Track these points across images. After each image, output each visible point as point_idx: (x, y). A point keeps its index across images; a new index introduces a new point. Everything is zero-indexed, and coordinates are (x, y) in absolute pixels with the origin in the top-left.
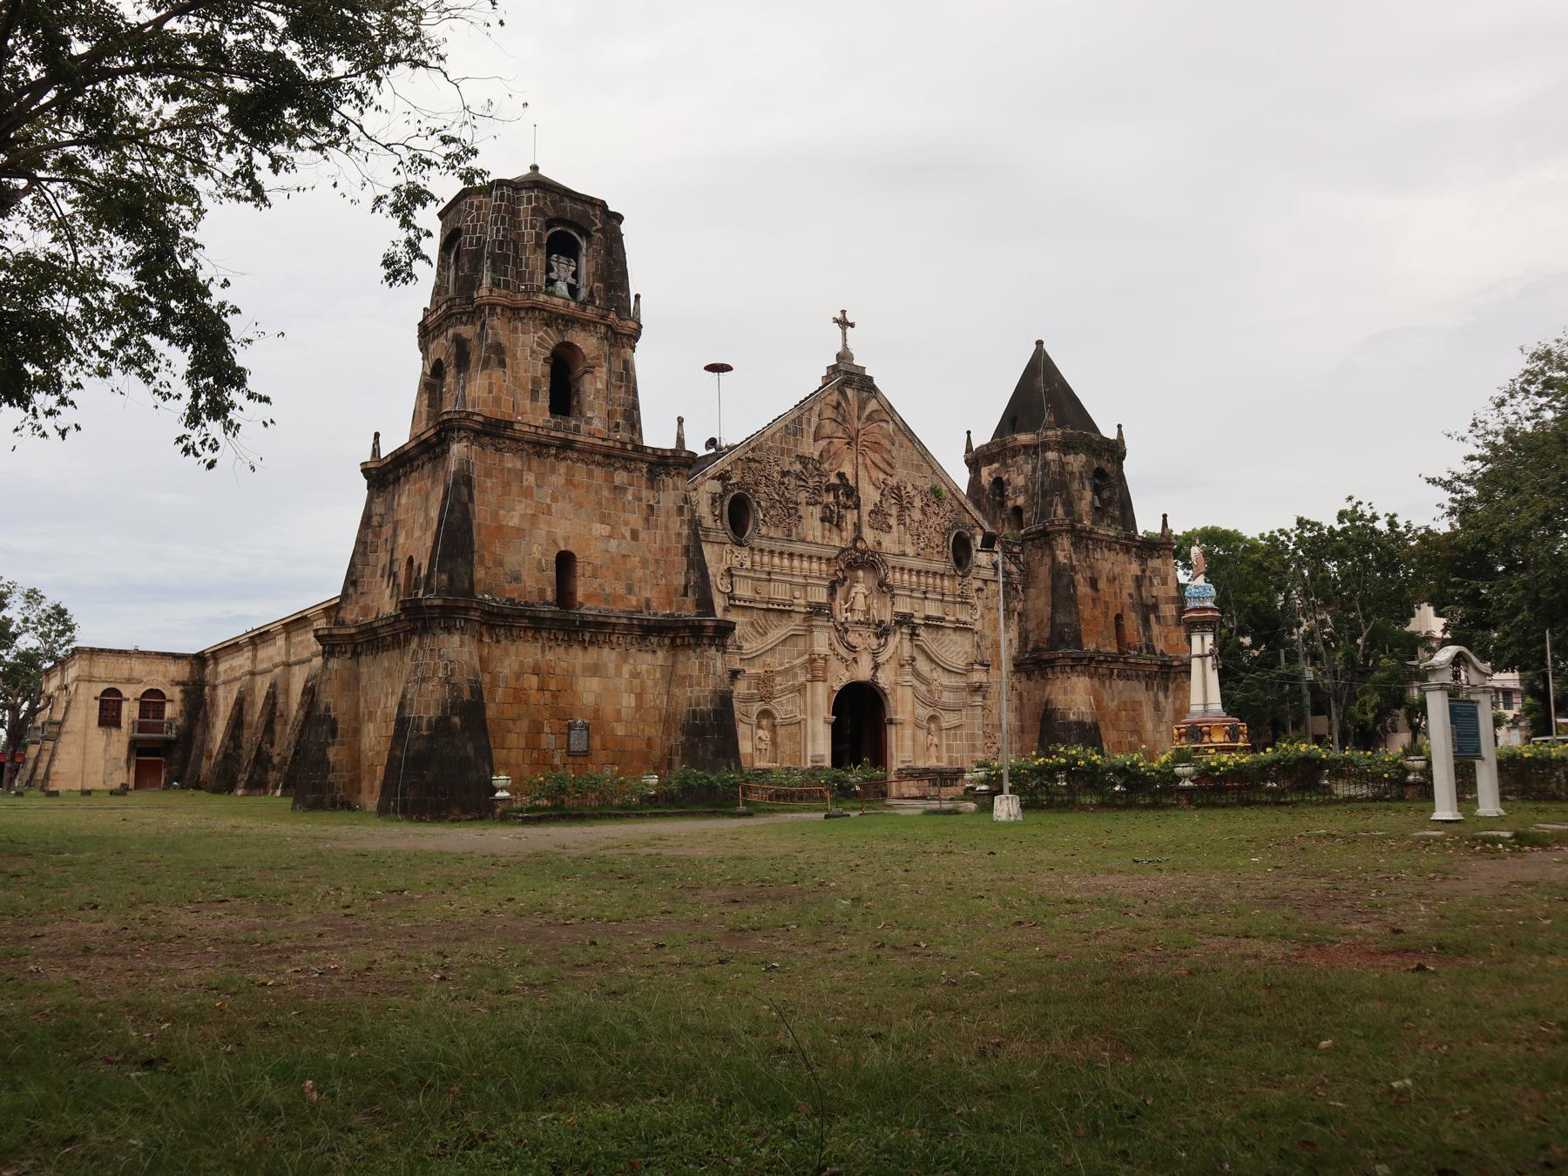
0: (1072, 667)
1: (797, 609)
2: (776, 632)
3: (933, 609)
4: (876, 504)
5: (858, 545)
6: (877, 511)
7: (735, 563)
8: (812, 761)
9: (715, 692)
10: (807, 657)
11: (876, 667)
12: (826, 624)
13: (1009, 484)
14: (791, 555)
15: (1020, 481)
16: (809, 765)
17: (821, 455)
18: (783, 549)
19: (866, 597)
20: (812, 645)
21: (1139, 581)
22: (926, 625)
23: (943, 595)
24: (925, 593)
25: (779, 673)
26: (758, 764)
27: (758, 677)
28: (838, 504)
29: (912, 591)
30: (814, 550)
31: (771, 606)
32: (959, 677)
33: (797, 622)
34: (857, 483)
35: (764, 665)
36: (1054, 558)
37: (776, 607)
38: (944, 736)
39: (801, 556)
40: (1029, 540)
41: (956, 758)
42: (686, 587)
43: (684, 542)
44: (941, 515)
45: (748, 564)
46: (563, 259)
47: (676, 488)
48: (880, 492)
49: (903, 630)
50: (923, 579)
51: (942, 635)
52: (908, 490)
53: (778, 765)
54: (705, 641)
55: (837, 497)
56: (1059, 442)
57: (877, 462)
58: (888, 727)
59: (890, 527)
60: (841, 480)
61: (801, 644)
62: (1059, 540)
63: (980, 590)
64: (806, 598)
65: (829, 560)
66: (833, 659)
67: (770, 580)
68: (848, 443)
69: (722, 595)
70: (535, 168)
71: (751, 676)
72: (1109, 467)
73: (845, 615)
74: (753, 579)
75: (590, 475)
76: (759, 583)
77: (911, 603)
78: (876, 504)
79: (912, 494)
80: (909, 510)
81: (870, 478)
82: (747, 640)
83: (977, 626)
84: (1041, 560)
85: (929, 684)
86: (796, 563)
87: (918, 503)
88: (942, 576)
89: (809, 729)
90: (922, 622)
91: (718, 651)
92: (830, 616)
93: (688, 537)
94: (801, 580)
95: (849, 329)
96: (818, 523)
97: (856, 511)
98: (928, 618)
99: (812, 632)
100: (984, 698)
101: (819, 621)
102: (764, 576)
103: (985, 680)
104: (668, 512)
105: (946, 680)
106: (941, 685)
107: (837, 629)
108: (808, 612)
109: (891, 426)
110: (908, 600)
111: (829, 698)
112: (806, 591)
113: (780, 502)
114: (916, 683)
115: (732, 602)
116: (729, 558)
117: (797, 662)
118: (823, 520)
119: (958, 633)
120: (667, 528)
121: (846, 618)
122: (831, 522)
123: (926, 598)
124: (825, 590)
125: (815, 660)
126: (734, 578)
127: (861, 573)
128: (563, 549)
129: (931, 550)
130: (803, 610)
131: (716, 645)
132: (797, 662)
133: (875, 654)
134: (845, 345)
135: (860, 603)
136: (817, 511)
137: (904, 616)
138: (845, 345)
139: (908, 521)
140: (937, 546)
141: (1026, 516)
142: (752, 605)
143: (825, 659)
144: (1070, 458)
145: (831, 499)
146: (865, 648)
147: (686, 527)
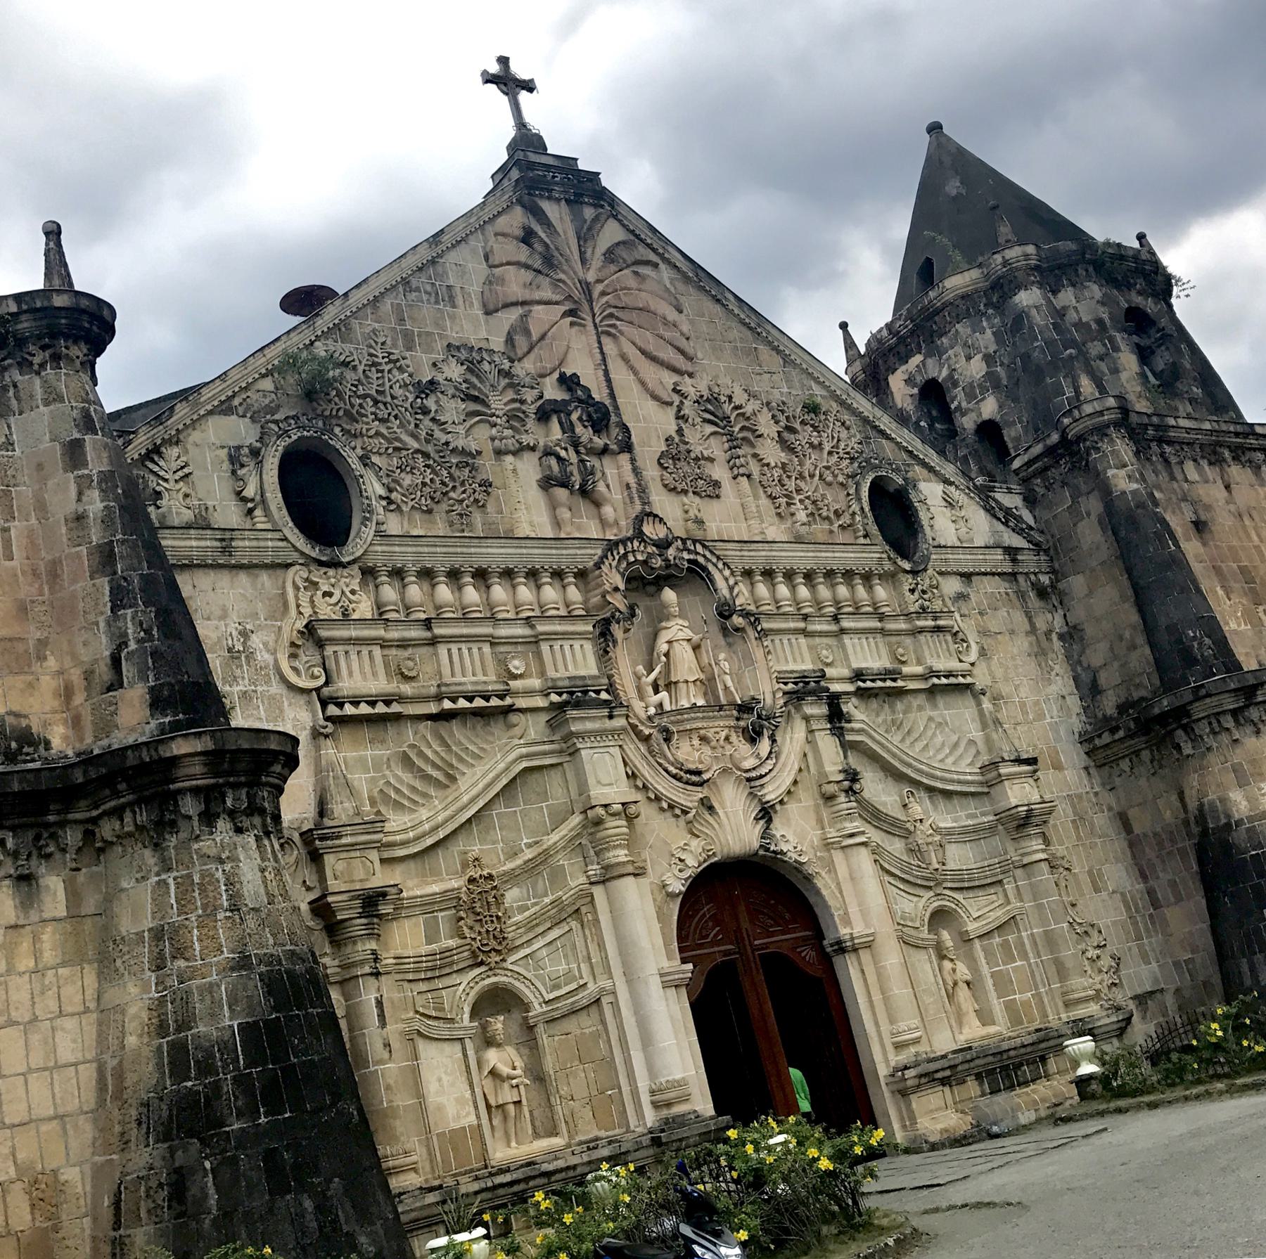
0: (1235, 713)
2: (479, 770)
5: (648, 529)
6: (674, 453)
8: (656, 1105)
9: (243, 963)
10: (576, 819)
11: (766, 813)
12: (609, 724)
13: (955, 384)
14: (481, 575)
15: (976, 369)
16: (651, 1118)
17: (510, 341)
18: (457, 562)
19: (696, 648)
20: (583, 788)
22: (862, 694)
23: (882, 617)
24: (836, 618)
25: (512, 877)
26: (501, 1153)
27: (450, 900)
28: (576, 444)
30: (537, 556)
31: (447, 704)
32: (972, 802)
33: (532, 734)
34: (612, 395)
35: (465, 865)
36: (1105, 490)
37: (462, 703)
38: (980, 955)
39: (508, 574)
40: (1034, 475)
41: (1026, 1004)
42: (116, 662)
43: (96, 535)
44: (827, 447)
45: (364, 607)
47: (52, 397)
48: (671, 412)
49: (809, 710)
50: (824, 592)
51: (905, 712)
52: (737, 401)
53: (557, 1142)
54: (190, 806)
55: (568, 428)
56: (1037, 268)
57: (650, 348)
58: (837, 961)
59: (717, 484)
60: (570, 389)
61: (556, 790)
62: (1105, 446)
63: (961, 597)
64: (542, 673)
65: (581, 575)
66: (647, 812)
67: (433, 642)
68: (571, 313)
69: (302, 700)
71: (429, 905)
72: (1150, 306)
73: (655, 699)
74: (384, 644)
76: (406, 653)
77: (811, 648)
78: (668, 440)
79: (748, 409)
80: (753, 446)
81: (643, 383)
82: (398, 806)
83: (980, 679)
84: (1074, 509)
85: (906, 834)
86: (499, 592)
88: (867, 578)
89: (626, 1012)
90: (850, 688)
91: (239, 831)
92: (613, 706)
93: (107, 521)
94: (520, 631)
95: (523, 96)
96: (534, 495)
97: (624, 458)
98: (859, 675)
99: (575, 752)
100: (1047, 842)
101: (583, 722)
102: (416, 633)
103: (1036, 797)
104: (40, 467)
105: (946, 818)
106: (937, 830)
107: (638, 734)
108: (554, 706)
109: (666, 273)
110: (802, 640)
111: (661, 917)
112: (539, 655)
113: (426, 455)
114: (875, 836)
116: (305, 602)
117: (554, 837)
118: (547, 483)
119: (941, 701)
120: (41, 507)
121: (661, 705)
122: (565, 484)
123: (843, 631)
124: (588, 646)
125: (598, 822)
126: (329, 650)
127: (669, 595)
129: (826, 526)
130: (540, 702)
131: (232, 814)
132: (554, 837)
133: (752, 781)
135: (686, 666)
137: (803, 678)
139: (754, 468)
140: (838, 514)
141: (1009, 434)
142: (395, 708)
143: (627, 813)
145: (556, 432)
146: (725, 771)
147: (96, 494)
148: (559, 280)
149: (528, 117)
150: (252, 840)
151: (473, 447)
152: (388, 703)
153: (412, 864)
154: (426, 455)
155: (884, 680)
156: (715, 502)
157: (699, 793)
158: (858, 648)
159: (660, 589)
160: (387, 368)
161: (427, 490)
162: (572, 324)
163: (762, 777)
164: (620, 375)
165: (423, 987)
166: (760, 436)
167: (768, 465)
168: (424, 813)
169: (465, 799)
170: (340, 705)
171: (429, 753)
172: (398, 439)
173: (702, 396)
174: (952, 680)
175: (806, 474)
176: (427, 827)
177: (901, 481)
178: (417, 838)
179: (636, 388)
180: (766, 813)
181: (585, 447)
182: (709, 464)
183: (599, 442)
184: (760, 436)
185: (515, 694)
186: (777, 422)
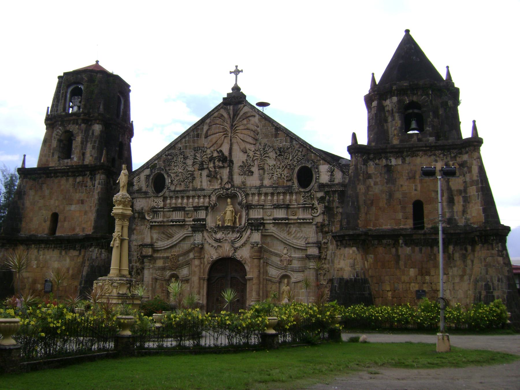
1: (188, 223)
2: (178, 235)
3: (280, 214)
4: (243, 162)
7: (155, 204)
28: (215, 167)
46: (76, 97)
55: (214, 163)
59: (253, 172)
70: (97, 62)
75: (67, 180)
78: (243, 162)
90: (271, 222)
98: (275, 219)
110: (261, 210)
115: (151, 224)
118: (208, 176)
127: (229, 200)
128: (54, 212)
134: (236, 84)
136: (205, 173)
138: (236, 84)
142: (162, 224)
144: (388, 102)
148: (225, 126)
149: (238, 83)
150: (97, 249)
151: (193, 169)
152: (161, 223)
154: (182, 173)
155: (281, 221)
156: (251, 177)
157: (219, 244)
158: (278, 212)
159: (228, 198)
160: (179, 155)
161: (181, 180)
162: (225, 137)
163: (235, 242)
164: (235, 147)
165: (160, 271)
166: (270, 158)
167: (269, 166)
168: (166, 242)
169: (174, 240)
170: (152, 223)
171: (168, 232)
172: (177, 170)
173: (255, 150)
174: (305, 221)
175: (281, 167)
176: (165, 245)
178: (163, 247)
179: (238, 149)
180: (236, 249)
181: (217, 167)
184: (270, 158)
185: (187, 221)
186: (277, 154)
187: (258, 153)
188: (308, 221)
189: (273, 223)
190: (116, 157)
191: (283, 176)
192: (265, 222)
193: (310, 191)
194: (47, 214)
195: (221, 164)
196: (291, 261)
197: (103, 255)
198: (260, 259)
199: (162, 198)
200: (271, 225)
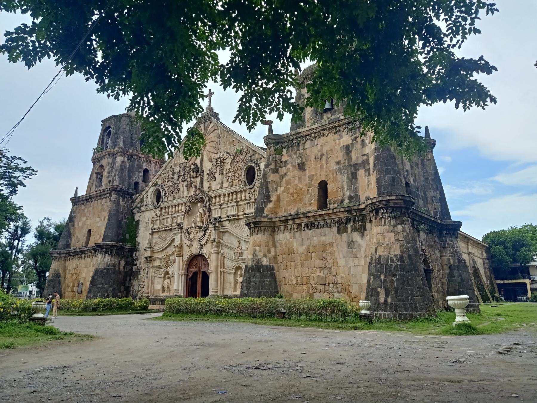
3: (232, 212)
4: (210, 170)
11: (201, 247)
21: (347, 150)
28: (190, 178)
29: (221, 205)
71: (161, 258)
78: (210, 170)
87: (229, 160)
98: (228, 217)
123: (228, 207)
127: (199, 204)
136: (185, 183)
153: (160, 253)
174: (249, 215)
177: (253, 165)
180: (201, 247)
182: (216, 173)
183: (195, 175)
187: (219, 160)
188: (251, 215)
189: (228, 220)
190: (140, 181)
191: (236, 178)
192: (222, 220)
193: (253, 187)
194: (85, 232)
195: (195, 175)
196: (242, 253)
197: (106, 259)
198: (218, 253)
199: (159, 209)
200: (228, 222)
